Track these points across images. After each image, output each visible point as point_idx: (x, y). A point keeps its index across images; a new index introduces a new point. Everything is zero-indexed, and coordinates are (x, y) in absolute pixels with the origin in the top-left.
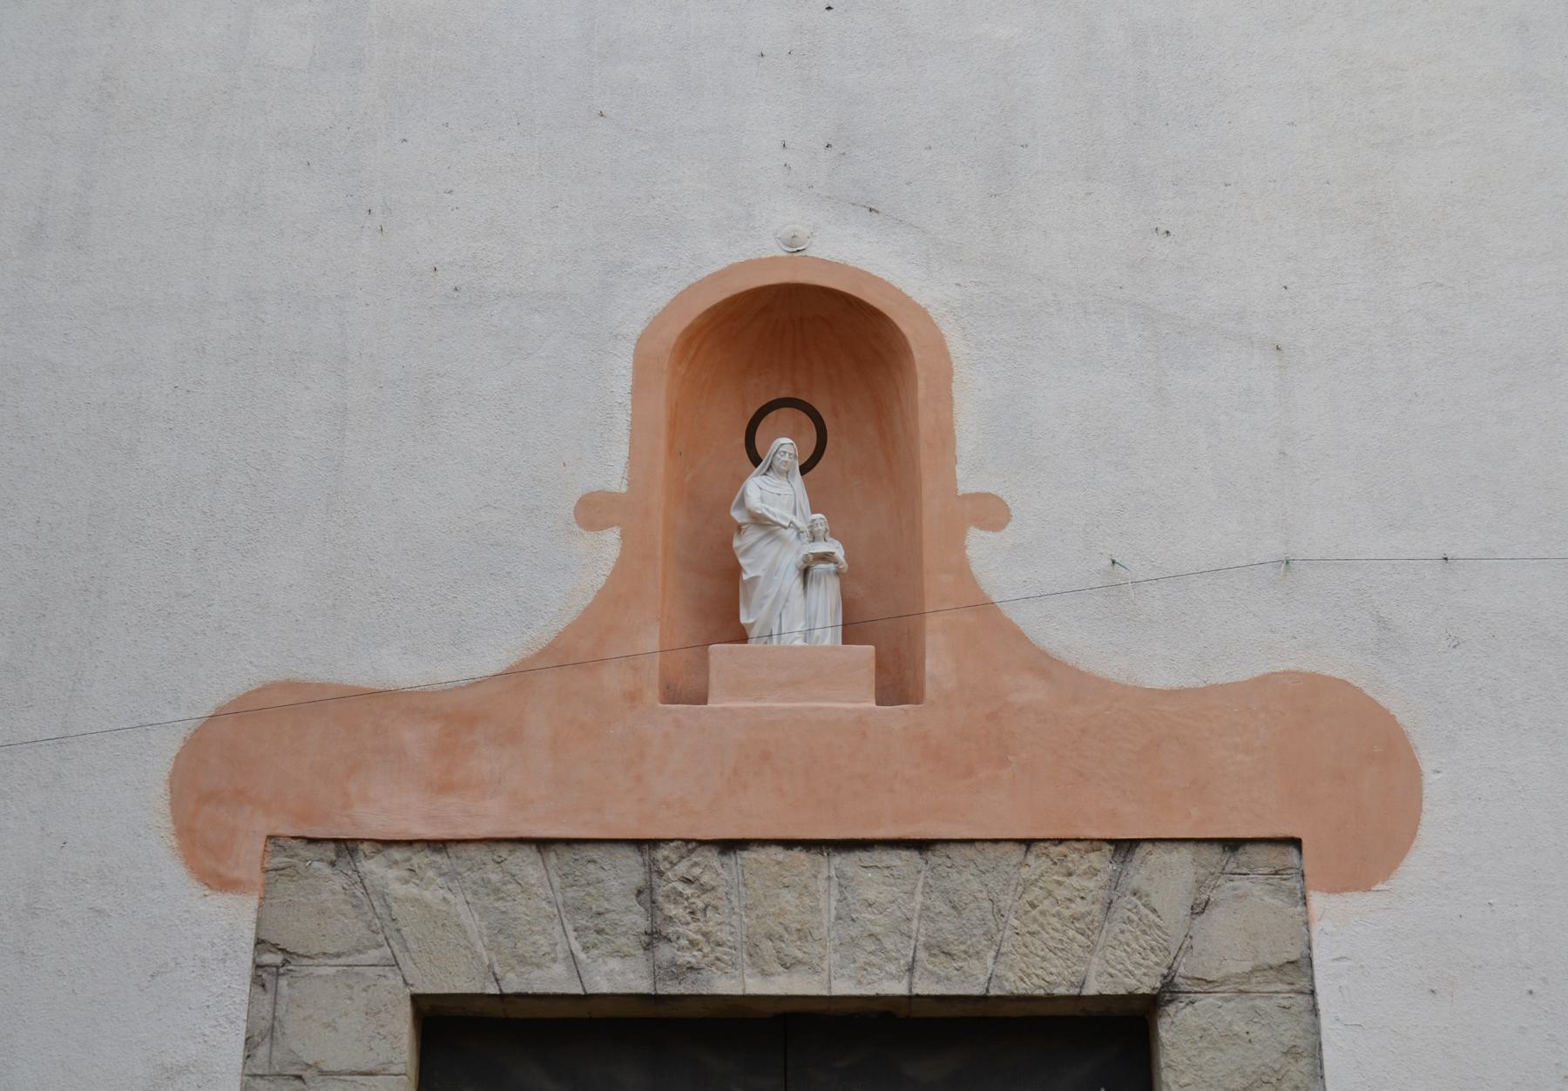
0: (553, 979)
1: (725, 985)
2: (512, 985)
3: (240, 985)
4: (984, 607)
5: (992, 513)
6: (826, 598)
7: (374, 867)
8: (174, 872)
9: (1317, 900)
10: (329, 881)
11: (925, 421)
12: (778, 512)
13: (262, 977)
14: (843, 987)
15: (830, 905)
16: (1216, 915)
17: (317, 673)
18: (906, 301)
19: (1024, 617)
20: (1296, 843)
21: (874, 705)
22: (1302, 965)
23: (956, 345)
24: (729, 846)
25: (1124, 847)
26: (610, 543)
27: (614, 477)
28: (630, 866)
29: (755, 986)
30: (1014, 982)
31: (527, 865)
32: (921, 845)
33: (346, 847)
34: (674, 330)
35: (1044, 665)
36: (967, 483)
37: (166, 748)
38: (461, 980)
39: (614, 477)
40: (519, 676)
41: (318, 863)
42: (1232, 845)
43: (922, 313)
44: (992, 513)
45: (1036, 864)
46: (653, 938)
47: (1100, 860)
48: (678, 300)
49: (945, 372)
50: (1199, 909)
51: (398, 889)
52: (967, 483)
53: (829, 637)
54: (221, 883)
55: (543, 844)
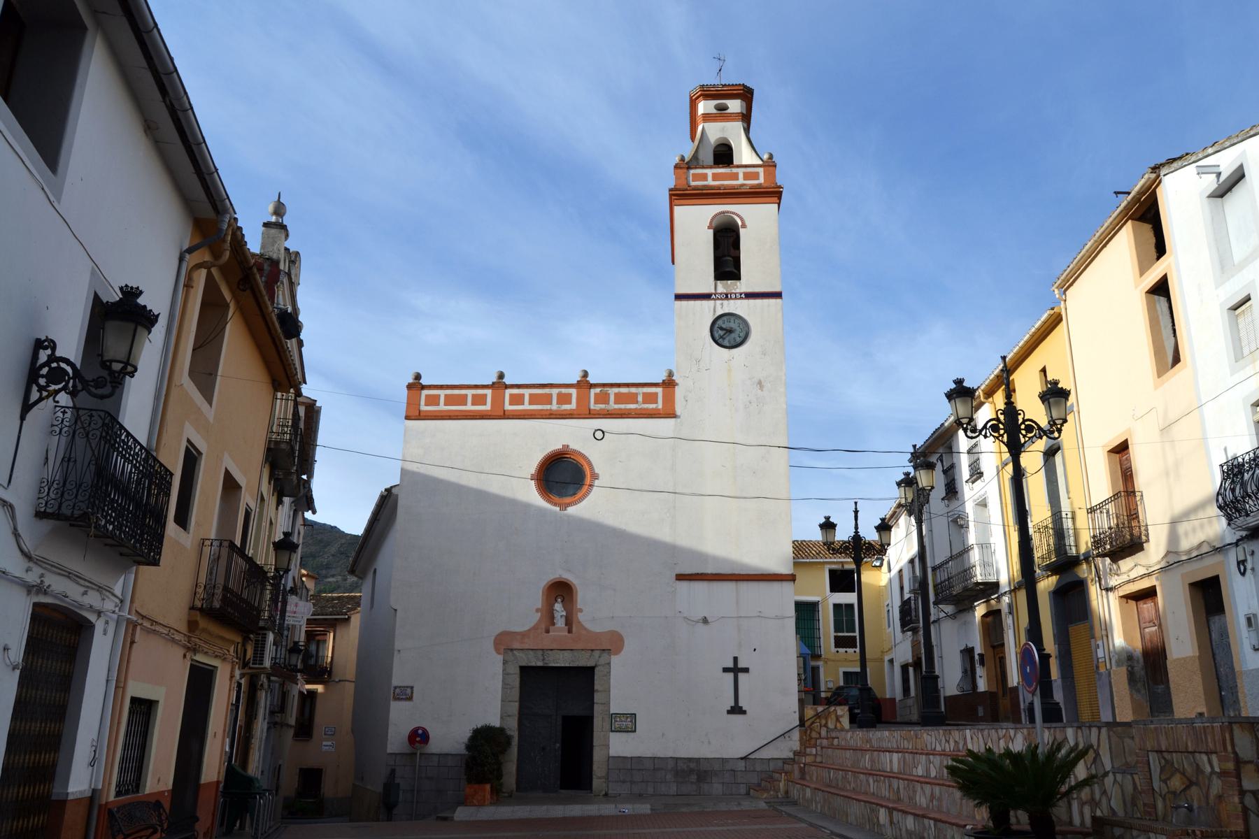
0: (533, 664)
1: (550, 665)
2: (530, 665)
3: (501, 664)
4: (579, 622)
5: (581, 610)
6: (563, 620)
7: (515, 652)
8: (494, 652)
9: (612, 656)
10: (510, 653)
11: (574, 599)
12: (558, 609)
13: (504, 663)
14: (563, 665)
15: (561, 656)
16: (602, 658)
17: (508, 630)
18: (572, 583)
19: (584, 624)
20: (610, 650)
21: (567, 634)
22: (609, 664)
23: (579, 590)
24: (552, 650)
25: (592, 650)
26: (539, 614)
27: (540, 606)
28: (541, 652)
29: (554, 665)
30: (580, 665)
31: (531, 652)
32: (572, 650)
33: (512, 650)
34: (546, 588)
35: (585, 629)
36: (579, 607)
37: (493, 638)
38: (524, 664)
39: (540, 606)
40: (529, 630)
41: (509, 652)
42: (604, 650)
43: (574, 585)
44: (581, 610)
45: (583, 652)
46: (543, 660)
47: (590, 651)
48: (547, 584)
49: (577, 592)
50: (599, 657)
51: (518, 654)
52: (579, 607)
53: (563, 625)
54: (499, 654)
55: (532, 649)
